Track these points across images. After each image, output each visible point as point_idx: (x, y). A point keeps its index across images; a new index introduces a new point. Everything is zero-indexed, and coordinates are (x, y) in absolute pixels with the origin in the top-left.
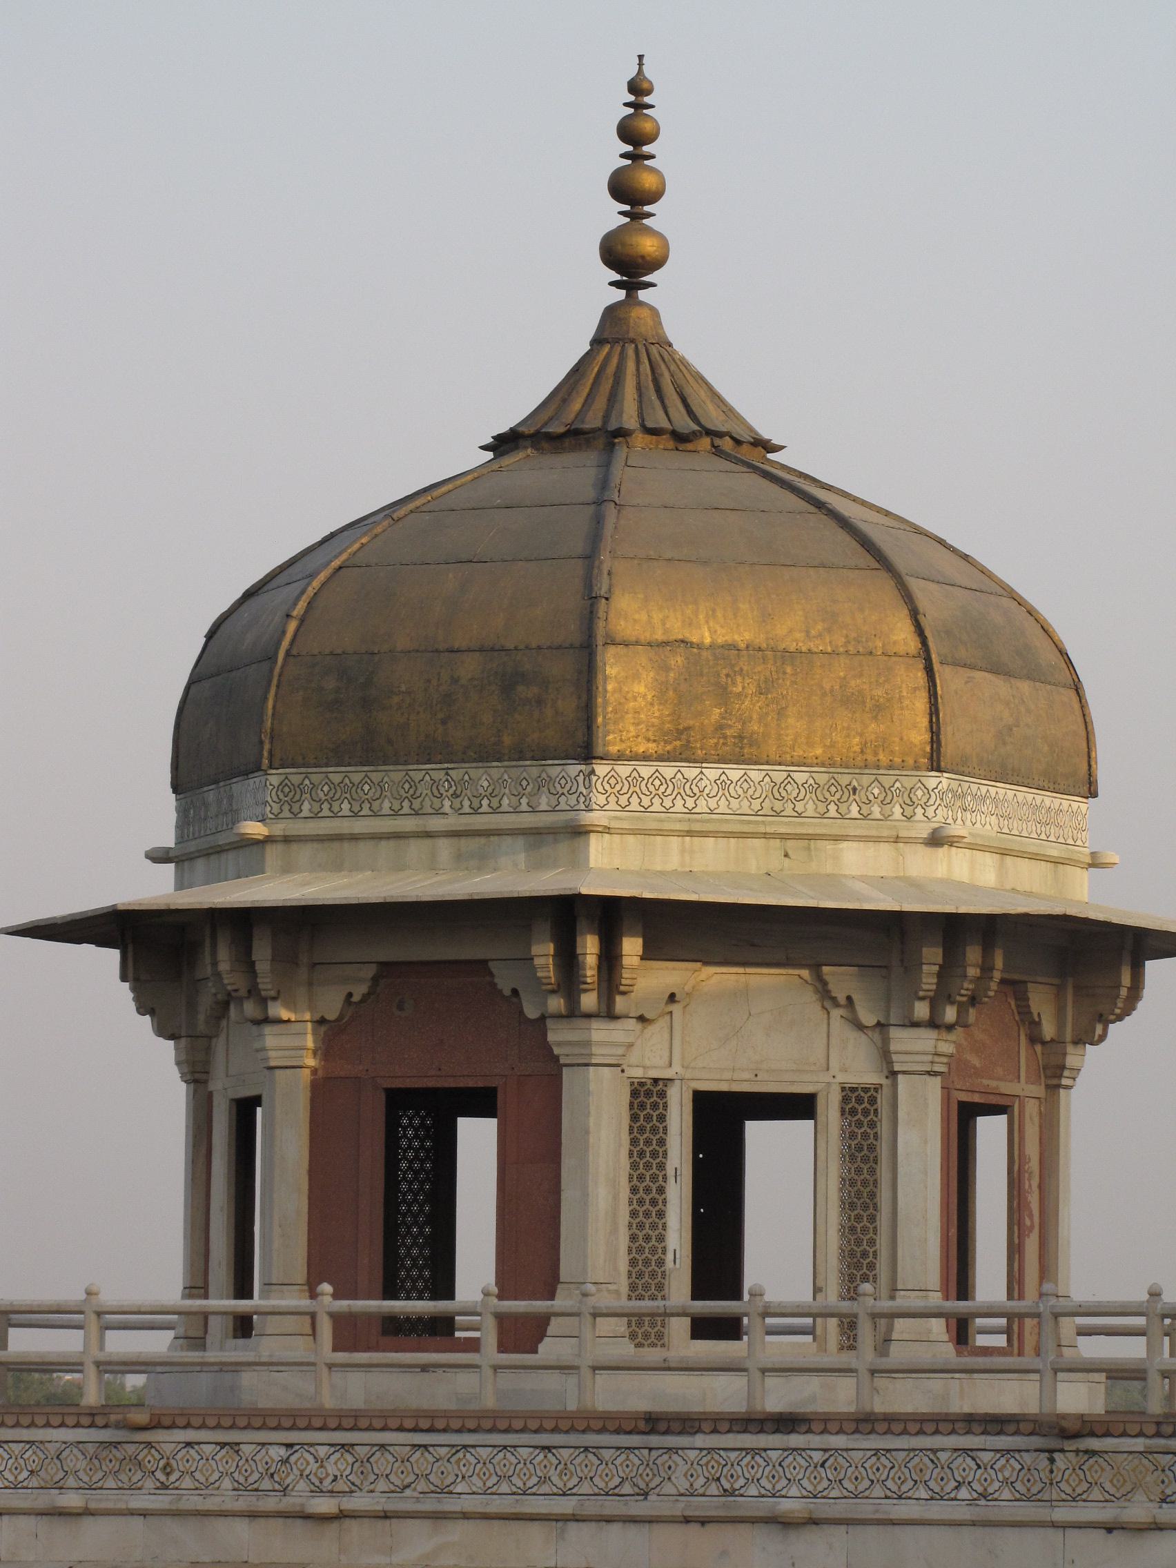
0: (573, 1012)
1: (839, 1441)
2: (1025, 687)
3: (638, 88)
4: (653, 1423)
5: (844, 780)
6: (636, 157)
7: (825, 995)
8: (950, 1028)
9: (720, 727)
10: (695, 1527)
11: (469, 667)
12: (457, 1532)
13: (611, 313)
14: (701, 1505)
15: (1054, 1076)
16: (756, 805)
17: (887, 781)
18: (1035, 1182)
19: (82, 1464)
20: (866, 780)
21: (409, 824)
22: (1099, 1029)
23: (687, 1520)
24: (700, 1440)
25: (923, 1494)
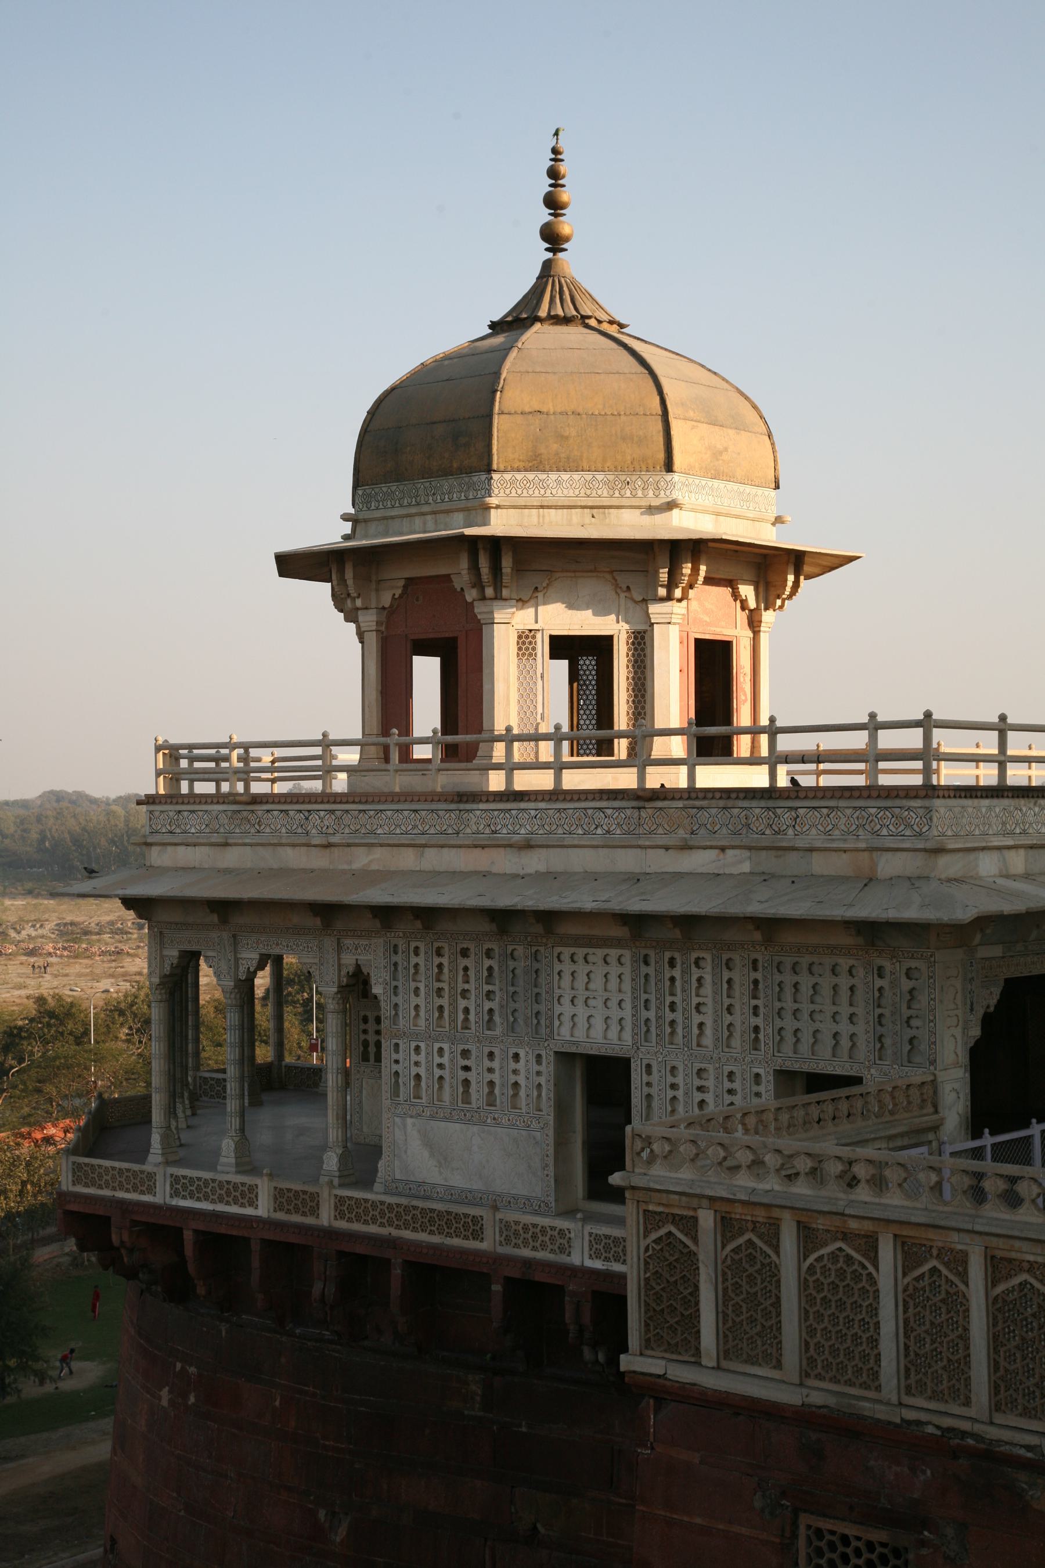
0: (484, 598)
1: (542, 805)
5: (623, 478)
7: (617, 586)
8: (680, 600)
9: (557, 454)
10: (478, 851)
12: (378, 853)
13: (547, 265)
16: (577, 492)
17: (645, 478)
18: (748, 678)
19: (226, 821)
20: (634, 478)
21: (413, 510)
22: (779, 602)
23: (476, 846)
24: (482, 806)
25: (580, 831)
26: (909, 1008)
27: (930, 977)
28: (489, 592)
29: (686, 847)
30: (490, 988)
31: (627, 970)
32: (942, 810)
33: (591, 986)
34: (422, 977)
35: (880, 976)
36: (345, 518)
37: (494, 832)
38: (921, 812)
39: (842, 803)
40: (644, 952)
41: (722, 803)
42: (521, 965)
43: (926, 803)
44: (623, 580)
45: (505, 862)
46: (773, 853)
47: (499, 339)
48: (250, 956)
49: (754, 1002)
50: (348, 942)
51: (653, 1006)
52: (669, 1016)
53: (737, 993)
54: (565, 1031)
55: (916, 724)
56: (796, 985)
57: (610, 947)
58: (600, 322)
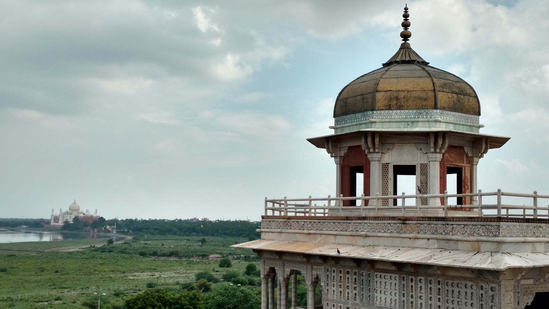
0: (370, 153)
1: (371, 222)
2: (462, 97)
3: (406, 9)
4: (347, 218)
6: (406, 20)
8: (440, 153)
11: (359, 98)
13: (402, 45)
14: (353, 233)
15: (472, 163)
18: (469, 181)
21: (350, 124)
22: (480, 155)
23: (351, 236)
24: (353, 221)
26: (492, 302)
27: (499, 291)
28: (371, 150)
29: (416, 238)
30: (356, 286)
31: (397, 282)
32: (504, 227)
33: (386, 287)
34: (335, 280)
35: (482, 289)
36: (331, 128)
37: (357, 231)
38: (496, 227)
39: (469, 223)
40: (403, 276)
41: (428, 222)
42: (364, 278)
43: (497, 223)
44: (420, 146)
45: (360, 241)
46: (445, 241)
47: (386, 68)
48: (288, 270)
49: (439, 297)
50: (314, 267)
51: (405, 295)
52: (411, 300)
53: (433, 293)
54: (378, 302)
55: (495, 194)
56: (453, 291)
57: (392, 273)
58: (419, 62)
